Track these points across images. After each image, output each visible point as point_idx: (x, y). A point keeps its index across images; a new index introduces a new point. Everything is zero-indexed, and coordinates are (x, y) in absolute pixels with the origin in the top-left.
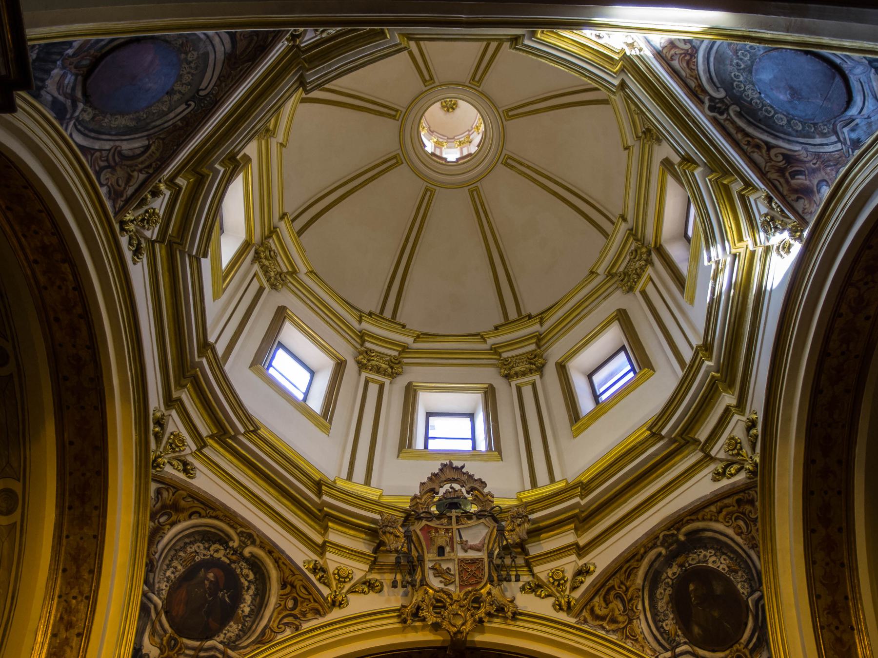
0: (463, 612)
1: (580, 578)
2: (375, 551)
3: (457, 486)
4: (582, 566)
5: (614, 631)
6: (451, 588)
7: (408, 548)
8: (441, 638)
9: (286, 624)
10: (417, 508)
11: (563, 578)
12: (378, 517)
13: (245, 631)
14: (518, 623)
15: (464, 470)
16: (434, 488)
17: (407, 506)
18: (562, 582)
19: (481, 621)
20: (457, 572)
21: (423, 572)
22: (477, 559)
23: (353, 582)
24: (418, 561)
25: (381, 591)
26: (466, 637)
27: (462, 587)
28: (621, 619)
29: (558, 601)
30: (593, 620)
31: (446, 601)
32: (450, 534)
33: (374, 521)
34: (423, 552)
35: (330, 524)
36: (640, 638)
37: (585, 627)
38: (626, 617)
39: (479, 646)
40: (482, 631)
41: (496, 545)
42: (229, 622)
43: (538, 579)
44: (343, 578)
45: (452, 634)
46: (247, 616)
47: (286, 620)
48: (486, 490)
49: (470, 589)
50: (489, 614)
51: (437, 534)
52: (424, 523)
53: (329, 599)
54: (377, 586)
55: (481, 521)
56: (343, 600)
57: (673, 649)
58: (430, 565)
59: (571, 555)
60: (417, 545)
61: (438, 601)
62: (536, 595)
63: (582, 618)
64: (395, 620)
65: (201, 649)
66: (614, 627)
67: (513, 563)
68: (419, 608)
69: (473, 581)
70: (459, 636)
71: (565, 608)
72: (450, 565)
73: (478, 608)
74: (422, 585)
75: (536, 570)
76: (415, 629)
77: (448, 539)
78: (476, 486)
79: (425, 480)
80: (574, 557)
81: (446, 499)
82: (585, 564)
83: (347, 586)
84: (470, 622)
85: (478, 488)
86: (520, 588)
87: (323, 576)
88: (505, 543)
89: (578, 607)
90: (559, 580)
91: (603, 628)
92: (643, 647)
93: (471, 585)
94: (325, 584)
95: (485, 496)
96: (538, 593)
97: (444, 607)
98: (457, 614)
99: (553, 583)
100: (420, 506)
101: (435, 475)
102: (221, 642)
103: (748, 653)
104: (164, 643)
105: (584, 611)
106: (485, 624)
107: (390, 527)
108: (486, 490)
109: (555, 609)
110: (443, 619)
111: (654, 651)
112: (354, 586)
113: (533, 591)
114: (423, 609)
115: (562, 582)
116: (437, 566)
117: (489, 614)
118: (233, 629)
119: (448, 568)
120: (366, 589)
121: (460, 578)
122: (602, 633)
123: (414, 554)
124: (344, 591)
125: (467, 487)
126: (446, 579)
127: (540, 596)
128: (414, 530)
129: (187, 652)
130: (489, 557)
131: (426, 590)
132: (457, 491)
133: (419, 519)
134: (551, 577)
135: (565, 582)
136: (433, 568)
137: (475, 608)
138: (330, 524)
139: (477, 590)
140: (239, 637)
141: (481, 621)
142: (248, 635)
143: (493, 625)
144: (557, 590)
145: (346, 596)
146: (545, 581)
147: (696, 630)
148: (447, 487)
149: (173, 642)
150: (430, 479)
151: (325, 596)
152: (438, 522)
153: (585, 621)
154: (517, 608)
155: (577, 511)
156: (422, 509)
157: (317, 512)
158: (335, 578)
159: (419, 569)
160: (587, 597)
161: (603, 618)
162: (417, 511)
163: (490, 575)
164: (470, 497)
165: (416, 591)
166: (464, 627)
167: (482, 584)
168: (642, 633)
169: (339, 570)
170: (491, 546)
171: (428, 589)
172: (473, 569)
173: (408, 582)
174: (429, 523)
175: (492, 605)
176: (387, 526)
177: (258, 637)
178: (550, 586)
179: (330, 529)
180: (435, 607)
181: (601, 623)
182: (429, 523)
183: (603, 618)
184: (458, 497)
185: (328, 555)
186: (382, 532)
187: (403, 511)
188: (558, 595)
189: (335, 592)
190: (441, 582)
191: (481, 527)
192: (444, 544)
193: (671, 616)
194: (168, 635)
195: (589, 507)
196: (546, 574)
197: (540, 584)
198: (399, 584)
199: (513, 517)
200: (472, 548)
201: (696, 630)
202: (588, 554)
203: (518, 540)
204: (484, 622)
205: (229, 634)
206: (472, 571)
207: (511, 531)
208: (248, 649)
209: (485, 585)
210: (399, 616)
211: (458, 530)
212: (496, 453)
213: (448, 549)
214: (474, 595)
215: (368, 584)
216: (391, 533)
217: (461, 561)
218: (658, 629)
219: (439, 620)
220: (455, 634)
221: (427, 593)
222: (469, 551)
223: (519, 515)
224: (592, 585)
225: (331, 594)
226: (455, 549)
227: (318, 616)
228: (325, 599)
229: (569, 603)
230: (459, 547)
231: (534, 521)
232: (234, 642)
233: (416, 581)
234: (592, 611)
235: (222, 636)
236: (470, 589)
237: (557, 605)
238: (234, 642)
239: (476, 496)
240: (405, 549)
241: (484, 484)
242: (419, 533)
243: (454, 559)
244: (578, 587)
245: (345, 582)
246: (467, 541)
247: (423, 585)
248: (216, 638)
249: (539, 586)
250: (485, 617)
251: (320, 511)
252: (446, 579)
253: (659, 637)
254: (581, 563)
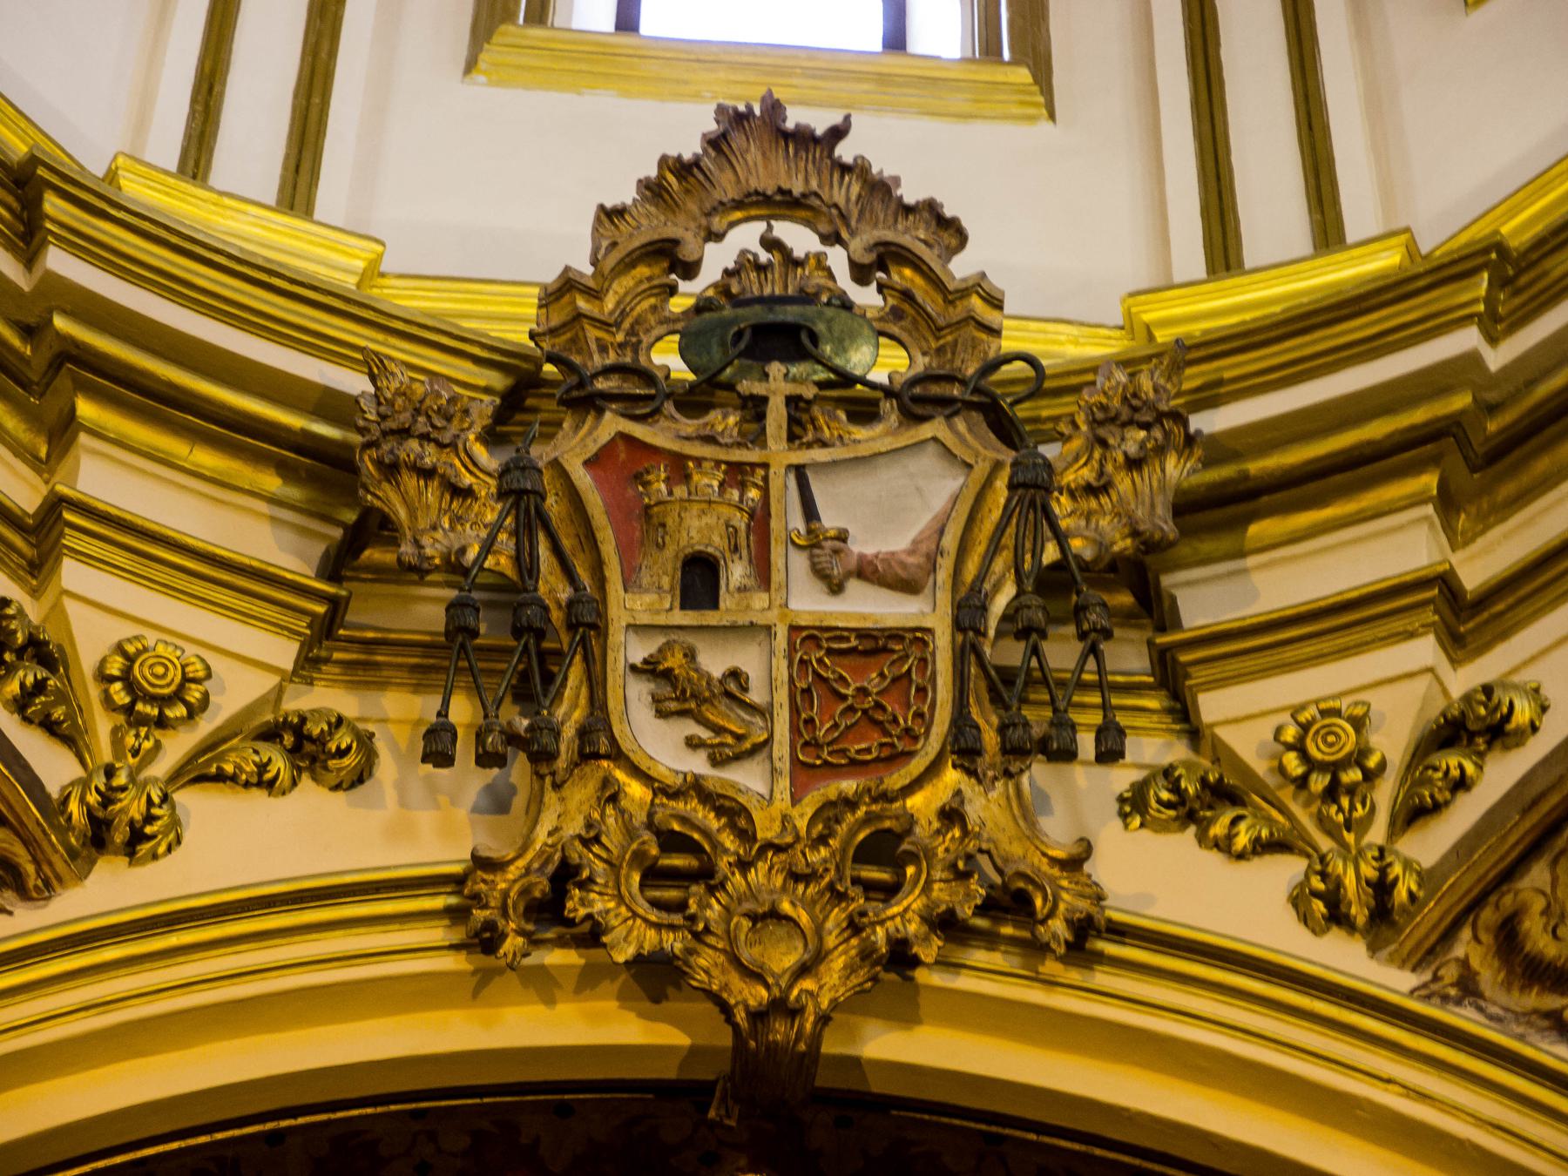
0: (810, 905)
1: (1452, 761)
2: (336, 565)
3: (799, 238)
4: (1467, 698)
6: (748, 779)
7: (517, 559)
8: (679, 1039)
10: (577, 343)
11: (1359, 757)
12: (354, 383)
14: (1103, 978)
15: (845, 151)
16: (675, 242)
17: (518, 336)
18: (1353, 775)
19: (901, 957)
20: (782, 696)
21: (596, 684)
22: (896, 634)
23: (206, 726)
24: (572, 627)
25: (360, 777)
26: (816, 1039)
27: (804, 773)
29: (1324, 876)
30: (1508, 985)
31: (716, 845)
32: (753, 494)
33: (330, 404)
34: (601, 581)
35: (86, 409)
37: (1464, 1018)
39: (877, 1086)
40: (906, 1011)
41: (999, 565)
43: (1221, 753)
44: (152, 699)
45: (740, 1016)
48: (961, 267)
49: (849, 786)
50: (946, 925)
51: (680, 491)
52: (612, 424)
53: (74, 807)
54: (342, 753)
55: (926, 431)
56: (150, 819)
58: (639, 651)
59: (1411, 635)
60: (567, 543)
61: (671, 842)
62: (1202, 839)
63: (1450, 973)
64: (436, 934)
67: (1091, 664)
68: (566, 875)
69: (867, 744)
70: (780, 1031)
71: (1359, 914)
72: (748, 659)
73: (889, 891)
74: (587, 756)
75: (1212, 706)
76: (544, 985)
77: (740, 520)
78: (906, 240)
79: (626, 194)
80: (1425, 650)
81: (737, 301)
82: (1488, 690)
83: (177, 747)
84: (838, 962)
85: (921, 250)
86: (1122, 800)
87: (40, 686)
88: (1051, 553)
89: (1432, 914)
90: (1335, 768)
93: (856, 765)
94: (50, 727)
95: (953, 296)
96: (1218, 829)
97: (706, 875)
98: (775, 915)
99: (1302, 782)
100: (593, 333)
101: (683, 169)
105: (1466, 933)
106: (921, 975)
107: (425, 438)
108: (961, 267)
109: (1305, 918)
110: (697, 936)
112: (211, 745)
113: (1190, 817)
114: (591, 880)
115: (1353, 775)
116: (674, 661)
117: (946, 925)
119: (735, 674)
120: (279, 765)
121: (795, 730)
123: (552, 587)
124: (161, 768)
125: (857, 244)
126: (718, 730)
127: (1223, 846)
128: (556, 464)
130: (958, 626)
131: (607, 782)
132: (798, 263)
133: (586, 402)
134: (1290, 747)
135: (1370, 776)
136: (650, 669)
137: (869, 887)
138: (86, 409)
139: (885, 797)
141: (901, 957)
143: (966, 982)
144: (1322, 821)
145: (165, 798)
146: (1260, 767)
148: (746, 236)
150: (653, 190)
151: (54, 790)
152: (689, 426)
153: (1468, 988)
154: (1099, 898)
155: (1461, 401)
156: (603, 349)
157: (16, 342)
158: (107, 700)
159: (575, 674)
160: (1487, 862)
162: (577, 359)
163: (961, 721)
164: (867, 297)
165: (557, 786)
166: (808, 984)
167: (917, 766)
169: (130, 659)
170: (971, 568)
171: (620, 775)
172: (873, 682)
173: (512, 739)
174: (639, 431)
175: (963, 876)
176: (404, 433)
178: (1286, 795)
179: (83, 438)
180: (653, 875)
182: (639, 431)
184: (806, 298)
185: (71, 574)
186: (379, 463)
187: (499, 357)
188: (1325, 844)
189: (110, 772)
190: (693, 743)
191: (928, 461)
192: (716, 543)
195: (1531, 383)
196: (1265, 729)
197: (1230, 780)
198: (464, 750)
199: (1105, 421)
200: (868, 572)
202: (1504, 635)
203: (1123, 544)
204: (916, 962)
206: (863, 692)
207: (1091, 490)
209: (933, 770)
210: (455, 915)
211: (800, 471)
212: (1023, 75)
213: (736, 572)
214: (869, 819)
215: (288, 740)
216: (427, 474)
217: (807, 636)
219: (674, 942)
220: (759, 1016)
221: (611, 796)
222: (853, 586)
223: (1134, 411)
224: (1521, 797)
225: (84, 784)
226: (777, 577)
228: (54, 809)
229: (1382, 887)
230: (799, 562)
231: (1219, 449)
233: (557, 734)
234: (1508, 937)
236: (849, 786)
237: (1316, 894)
239: (907, 295)
240: (501, 561)
241: (951, 232)
242: (583, 479)
243: (768, 629)
244: (1437, 808)
245: (161, 723)
246: (842, 536)
247: (597, 756)
249: (1222, 794)
250: (926, 939)
251: (29, 332)
252: (718, 730)
254: (1462, 680)
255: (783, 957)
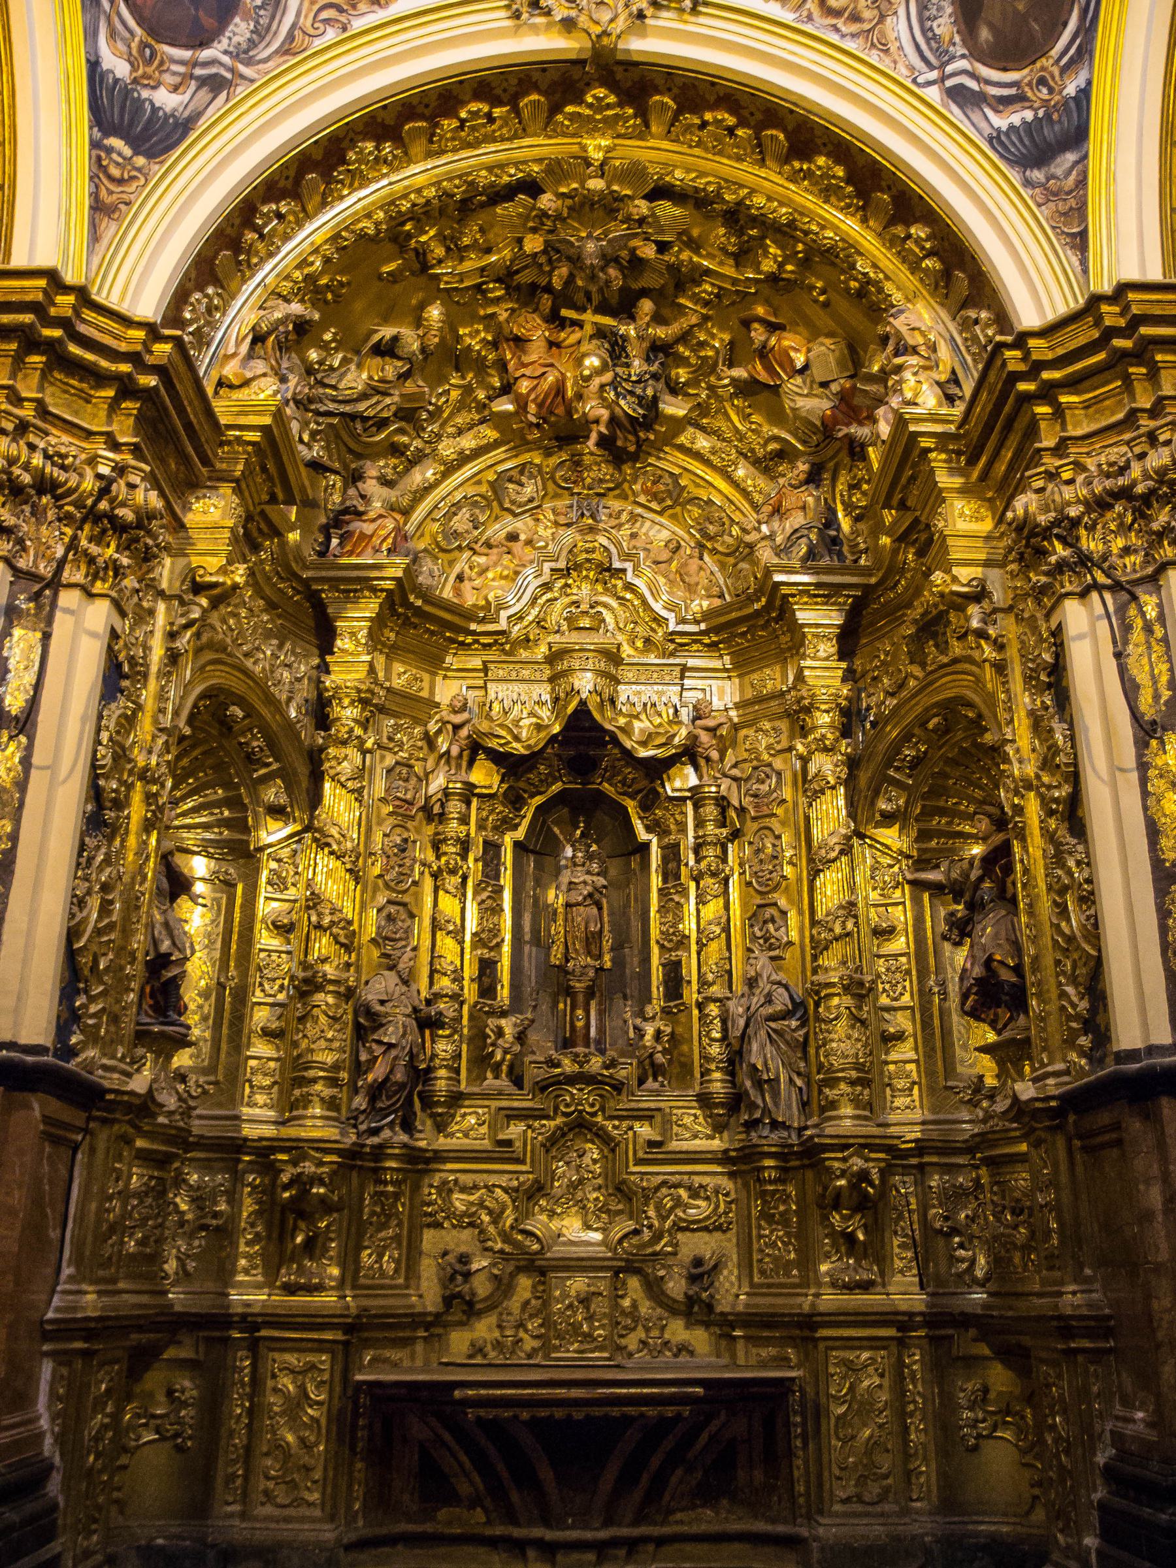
5: (853, 36)
8: (576, 45)
9: (327, 21)
13: (260, 34)
14: (702, 20)
28: (867, 14)
36: (893, 47)
37: (808, 28)
38: (876, 12)
39: (636, 58)
40: (643, 33)
42: (233, 18)
46: (260, 8)
47: (325, 15)
57: (943, 66)
63: (805, 13)
64: (503, 14)
65: (195, 64)
66: (854, 28)
70: (605, 41)
76: (535, 28)
84: (622, 18)
91: (836, 29)
92: (895, 62)
102: (226, 52)
103: (1056, 71)
104: (134, 52)
111: (912, 68)
118: (240, 29)
122: (834, 38)
129: (174, 68)
140: (252, 44)
141: (641, 15)
142: (268, 39)
143: (661, 23)
147: (985, 34)
149: (148, 51)
153: (810, 18)
161: (837, 13)
168: (898, 39)
177: (283, 44)
181: (834, 21)
183: (837, 13)
193: (949, 10)
194: (137, 39)
201: (985, 34)
204: (645, 17)
205: (236, 39)
208: (270, 64)
210: (508, 7)
218: (924, 32)
219: (573, 13)
220: (599, 36)
227: (376, 7)
232: (246, 52)
235: (225, 41)
238: (246, 52)
248: (215, 44)
253: (924, 46)
255: (605, 16)
